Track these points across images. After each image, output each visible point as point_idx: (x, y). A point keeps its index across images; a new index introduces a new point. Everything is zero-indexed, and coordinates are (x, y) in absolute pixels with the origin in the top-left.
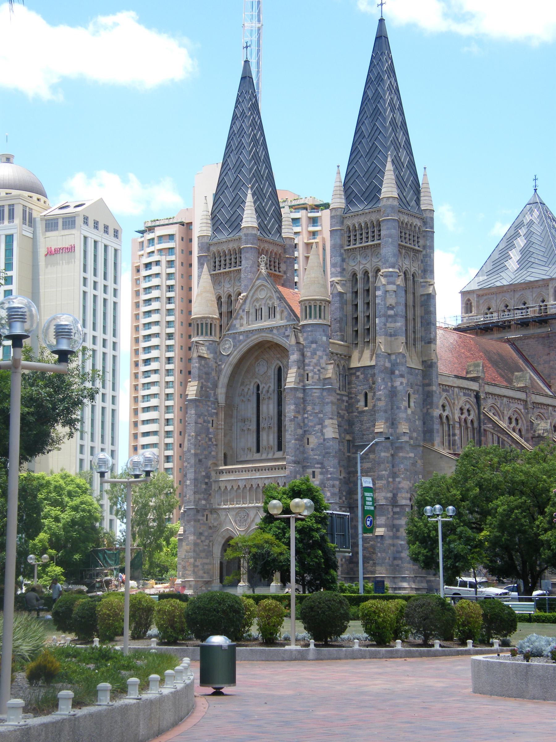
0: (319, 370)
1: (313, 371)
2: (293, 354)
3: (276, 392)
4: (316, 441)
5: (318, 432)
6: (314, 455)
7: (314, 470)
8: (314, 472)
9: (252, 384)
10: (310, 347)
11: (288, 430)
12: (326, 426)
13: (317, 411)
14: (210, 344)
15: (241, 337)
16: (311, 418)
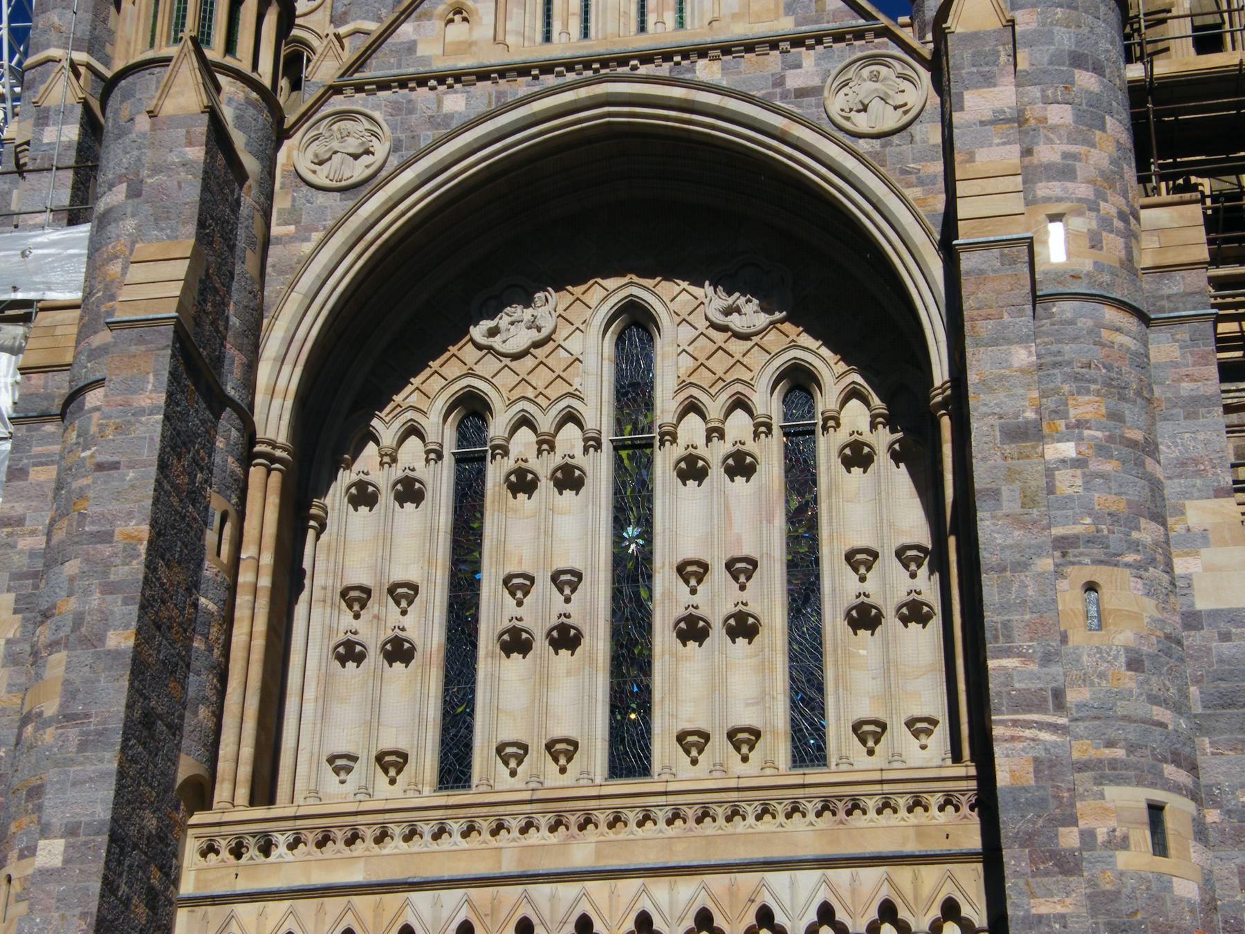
0: (1122, 216)
1: (1094, 207)
2: (988, 80)
3: (606, 446)
4: (1150, 604)
5: (1153, 561)
6: (1153, 700)
7: (1158, 795)
8: (1155, 811)
9: (441, 404)
10: (1068, 84)
11: (995, 494)
12: (1198, 540)
13: (1137, 435)
14: (248, 101)
15: (455, 102)
16: (1108, 467)
